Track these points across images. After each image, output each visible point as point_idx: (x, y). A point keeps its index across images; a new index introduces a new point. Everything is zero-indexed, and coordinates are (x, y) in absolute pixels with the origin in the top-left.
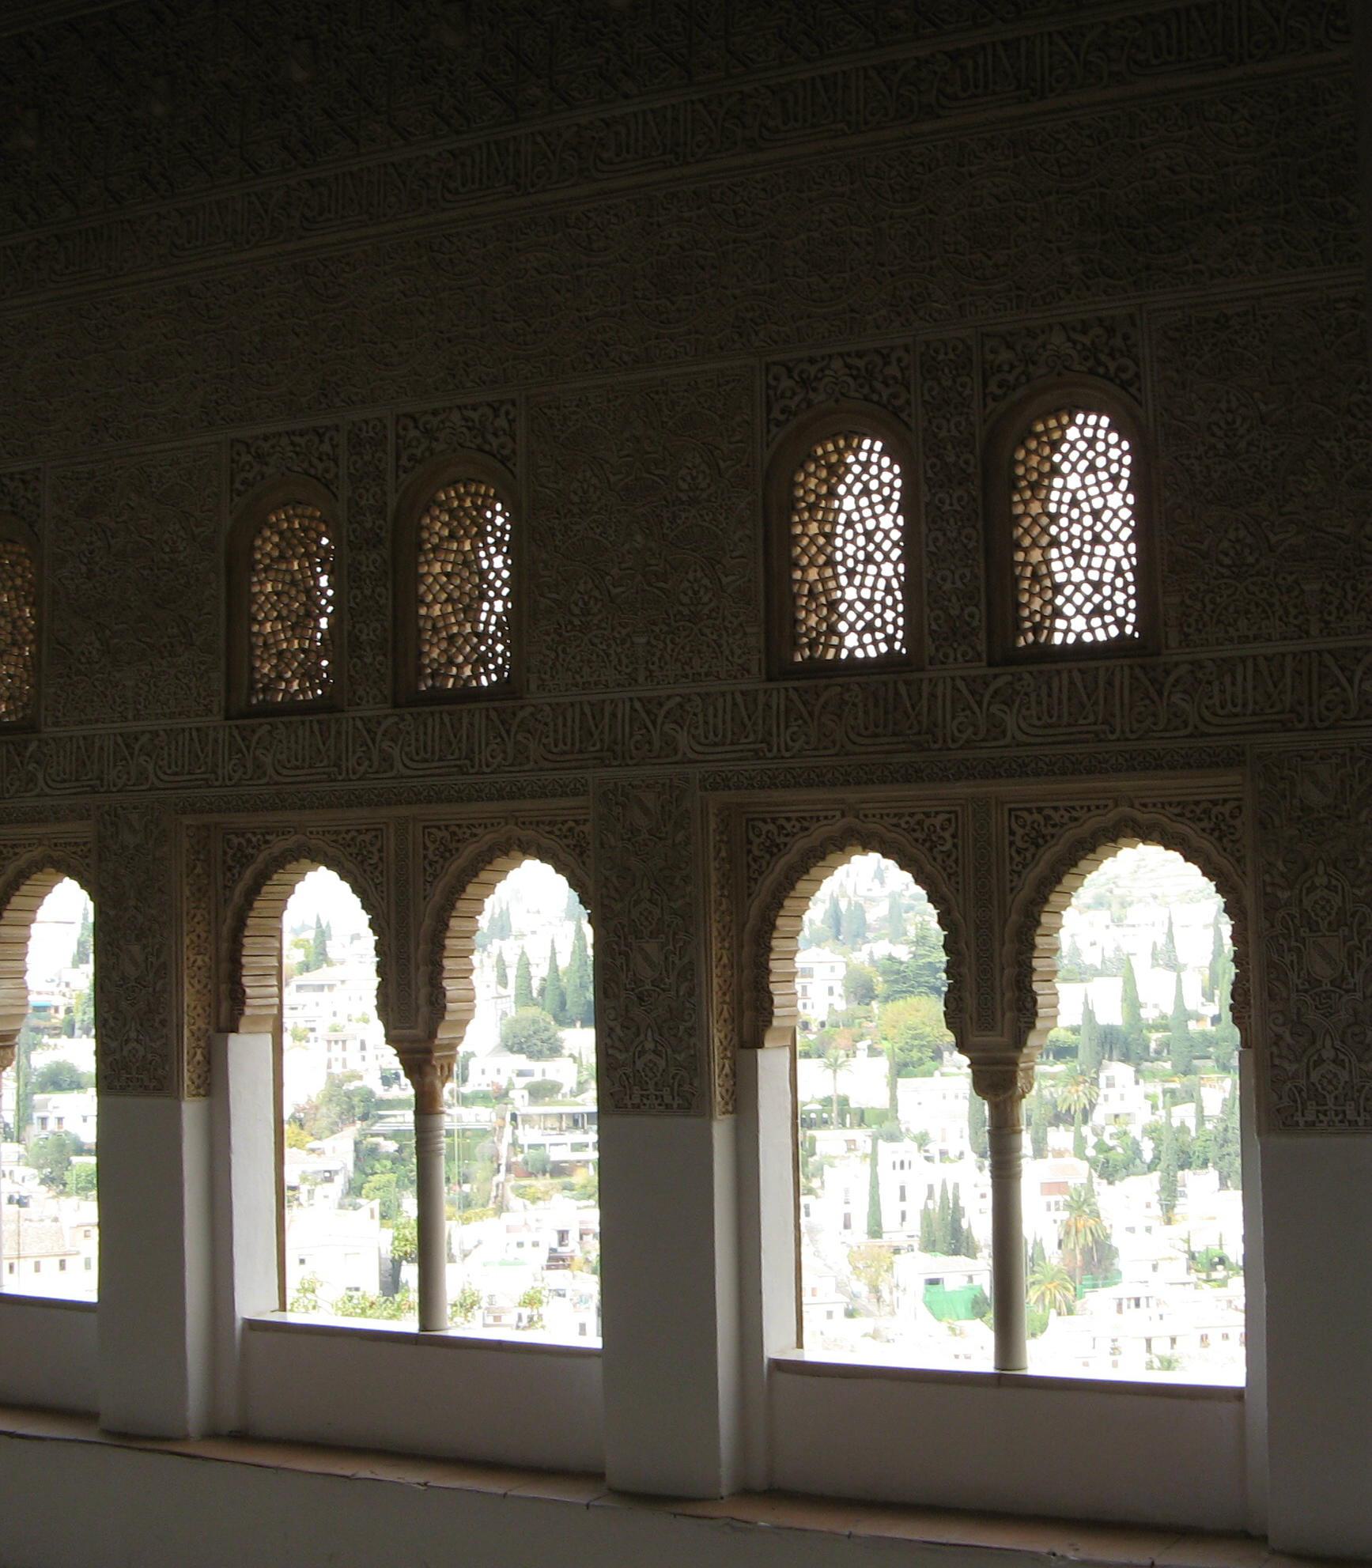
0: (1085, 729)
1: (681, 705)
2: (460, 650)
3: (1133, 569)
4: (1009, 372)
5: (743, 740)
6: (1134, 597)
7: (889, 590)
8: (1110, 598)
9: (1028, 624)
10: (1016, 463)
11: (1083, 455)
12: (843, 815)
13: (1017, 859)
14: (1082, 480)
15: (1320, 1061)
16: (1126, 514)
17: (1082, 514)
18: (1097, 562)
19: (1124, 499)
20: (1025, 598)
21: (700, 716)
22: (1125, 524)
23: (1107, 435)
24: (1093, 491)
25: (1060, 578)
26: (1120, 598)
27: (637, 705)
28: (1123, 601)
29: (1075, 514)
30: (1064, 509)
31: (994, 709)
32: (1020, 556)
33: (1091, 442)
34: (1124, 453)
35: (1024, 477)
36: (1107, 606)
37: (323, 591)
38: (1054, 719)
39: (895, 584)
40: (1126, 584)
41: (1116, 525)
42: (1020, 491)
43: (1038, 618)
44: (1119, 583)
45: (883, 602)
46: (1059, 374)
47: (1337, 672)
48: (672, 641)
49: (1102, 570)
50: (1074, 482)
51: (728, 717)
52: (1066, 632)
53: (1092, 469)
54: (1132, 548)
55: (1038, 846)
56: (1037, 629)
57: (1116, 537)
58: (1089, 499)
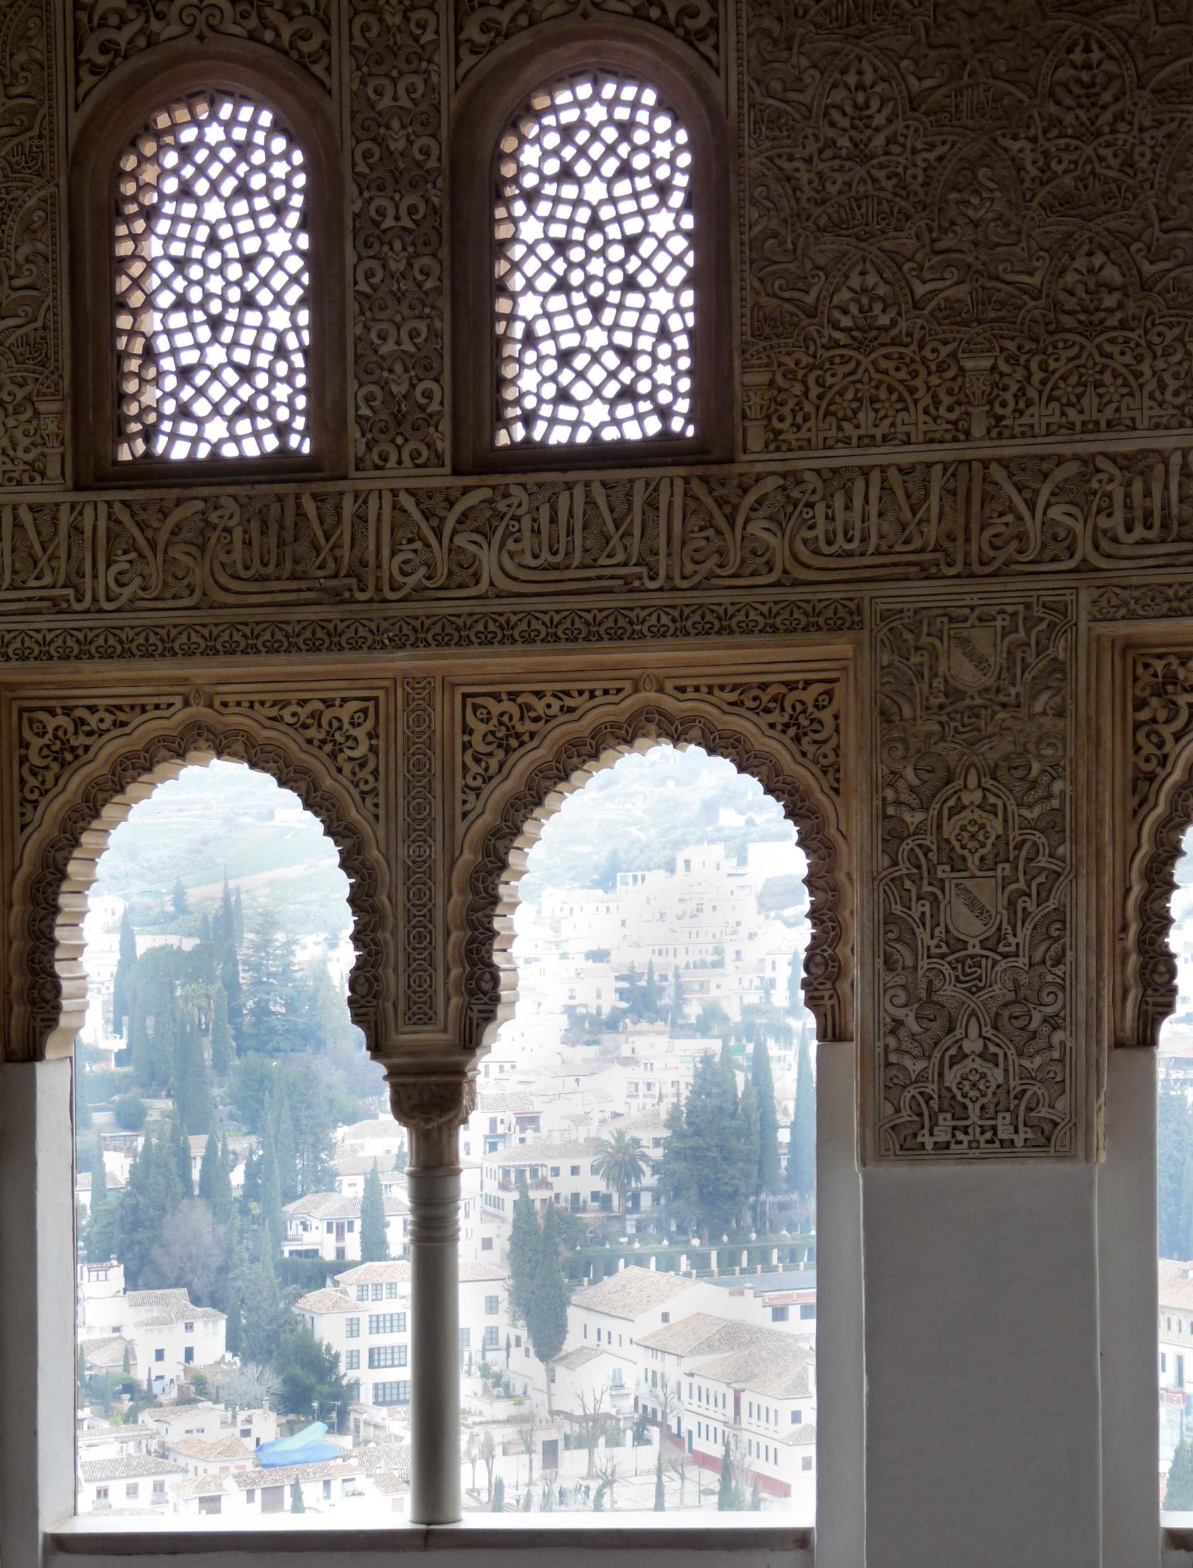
0: (38, 593)
6: (304, 391)
8: (266, 391)
9: (135, 427)
14: (227, 209)
16: (295, 264)
17: (226, 261)
18: (248, 337)
19: (293, 241)
20: (131, 386)
23: (268, 140)
24: (246, 226)
29: (214, 260)
30: (197, 251)
33: (243, 149)
34: (294, 170)
35: (134, 198)
36: (262, 403)
38: (271, 567)
40: (293, 371)
42: (128, 220)
43: (152, 418)
44: (282, 369)
46: (201, 37)
47: (136, 532)
49: (255, 348)
52: (196, 441)
53: (243, 191)
55: (63, 764)
58: (237, 238)
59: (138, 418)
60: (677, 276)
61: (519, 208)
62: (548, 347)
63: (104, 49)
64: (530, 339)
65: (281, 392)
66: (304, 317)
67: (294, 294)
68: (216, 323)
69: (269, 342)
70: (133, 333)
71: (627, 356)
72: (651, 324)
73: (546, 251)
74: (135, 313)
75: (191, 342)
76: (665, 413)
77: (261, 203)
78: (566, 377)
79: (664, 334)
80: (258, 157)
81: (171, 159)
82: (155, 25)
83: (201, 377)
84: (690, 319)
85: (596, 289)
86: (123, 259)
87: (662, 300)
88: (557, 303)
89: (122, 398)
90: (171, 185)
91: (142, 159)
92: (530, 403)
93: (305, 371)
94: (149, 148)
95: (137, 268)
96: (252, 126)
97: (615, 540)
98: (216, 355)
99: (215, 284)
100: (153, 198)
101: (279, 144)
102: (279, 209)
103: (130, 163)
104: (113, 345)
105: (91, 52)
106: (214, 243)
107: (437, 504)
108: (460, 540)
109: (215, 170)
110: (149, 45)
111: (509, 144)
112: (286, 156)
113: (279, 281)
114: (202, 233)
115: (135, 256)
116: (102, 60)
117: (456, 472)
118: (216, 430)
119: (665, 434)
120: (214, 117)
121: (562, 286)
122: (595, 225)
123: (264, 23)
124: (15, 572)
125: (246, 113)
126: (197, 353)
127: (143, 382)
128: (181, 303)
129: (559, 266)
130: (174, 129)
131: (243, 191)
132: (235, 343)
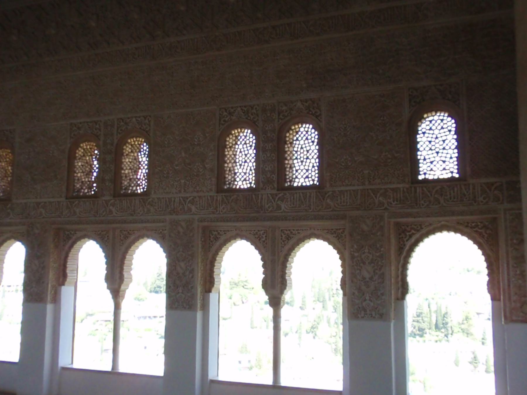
1: (193, 199)
2: (133, 183)
3: (254, 169)
4: (226, 118)
5: (210, 209)
11: (243, 140)
13: (211, 243)
15: (178, 293)
22: (253, 158)
25: (236, 171)
26: (251, 177)
27: (181, 199)
28: (252, 177)
31: (189, 205)
32: (226, 165)
37: (9, 170)
39: (145, 175)
41: (250, 158)
45: (142, 179)
48: (191, 182)
50: (241, 146)
54: (254, 164)
56: (229, 184)
57: (250, 161)
59: (289, 179)
60: (454, 147)
61: (422, 135)
62: (428, 161)
63: (283, 116)
64: (425, 159)
65: (313, 174)
66: (317, 160)
67: (315, 156)
68: (302, 162)
69: (311, 165)
70: (421, 155)
72: (449, 156)
74: (288, 160)
75: (298, 165)
76: (452, 172)
77: (310, 141)
78: (432, 166)
79: (451, 158)
80: (309, 133)
81: (295, 134)
83: (299, 171)
84: (456, 155)
85: (437, 150)
86: (419, 142)
87: (451, 151)
88: (430, 152)
89: (286, 175)
90: (295, 138)
91: (290, 134)
92: (425, 171)
93: (318, 170)
94: (291, 132)
95: (289, 153)
96: (308, 128)
98: (302, 167)
99: (302, 155)
100: (291, 141)
101: (313, 131)
102: (313, 142)
103: (288, 135)
104: (284, 166)
105: (281, 117)
106: (302, 148)
108: (436, 196)
109: (302, 135)
111: (419, 124)
112: (314, 133)
113: (313, 154)
114: (300, 146)
115: (289, 151)
116: (282, 117)
118: (302, 180)
119: (452, 177)
120: (302, 126)
121: (431, 149)
122: (437, 138)
125: (307, 126)
126: (299, 167)
127: (289, 172)
128: (296, 158)
129: (430, 146)
130: (295, 129)
131: (307, 139)
132: (305, 165)
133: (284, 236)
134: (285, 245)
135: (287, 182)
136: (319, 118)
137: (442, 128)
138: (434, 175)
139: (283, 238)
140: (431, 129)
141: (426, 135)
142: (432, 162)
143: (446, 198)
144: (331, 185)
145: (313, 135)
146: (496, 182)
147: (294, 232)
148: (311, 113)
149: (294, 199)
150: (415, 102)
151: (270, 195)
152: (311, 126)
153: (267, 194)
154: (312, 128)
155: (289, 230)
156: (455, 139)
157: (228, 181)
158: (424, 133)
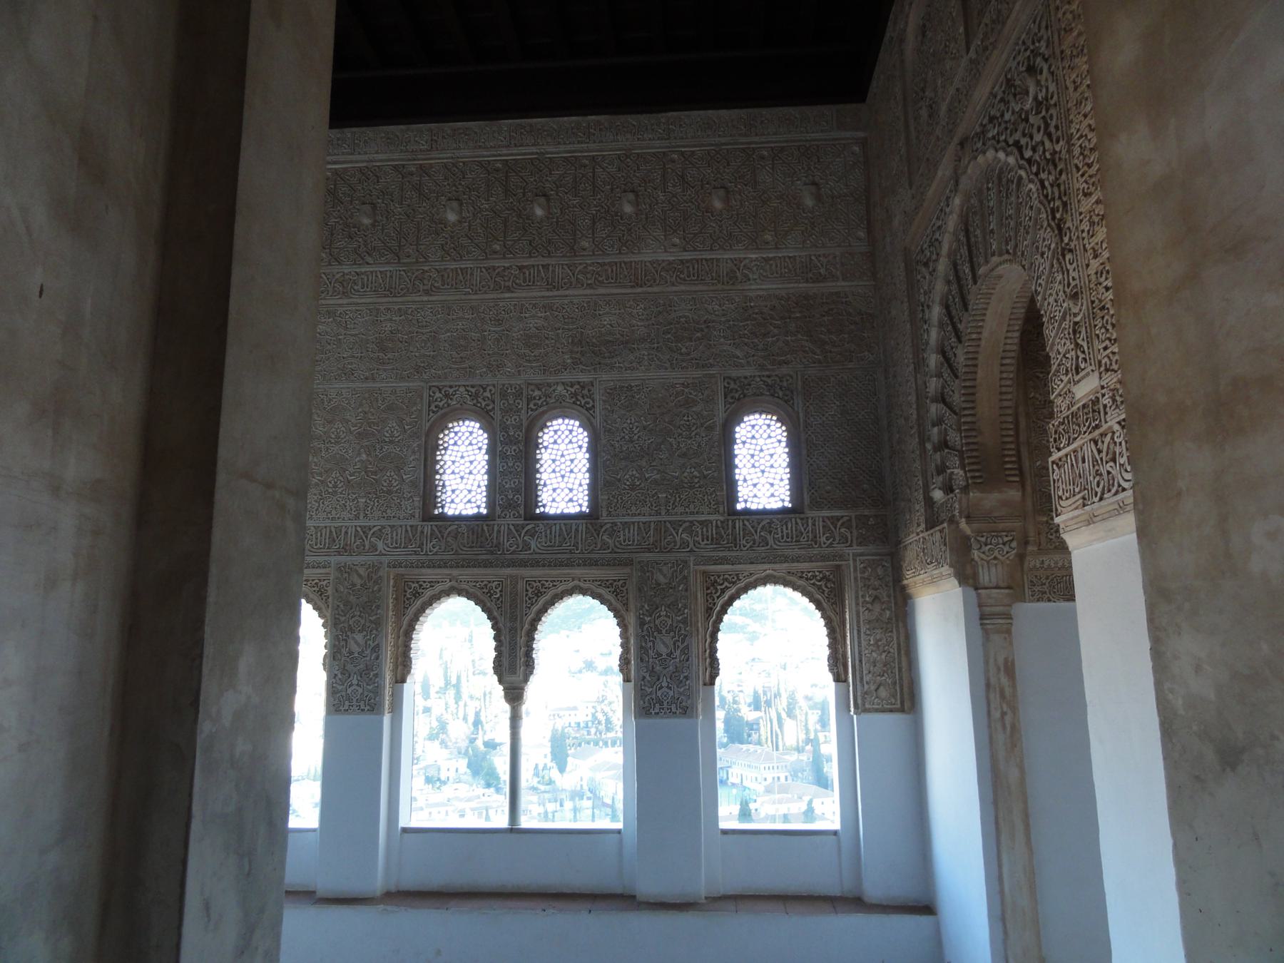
7: (479, 486)
10: (439, 439)
12: (450, 581)
13: (407, 602)
21: (390, 535)
48: (378, 501)
51: (403, 536)
61: (741, 446)
64: (745, 480)
71: (772, 485)
73: (749, 457)
76: (783, 501)
78: (755, 491)
79: (782, 480)
81: (552, 433)
82: (548, 399)
92: (746, 497)
97: (804, 535)
99: (563, 467)
102: (580, 447)
105: (531, 406)
107: (755, 524)
108: (762, 534)
110: (744, 396)
117: (729, 515)
121: (753, 466)
122: (761, 450)
123: (577, 400)
124: (797, 537)
129: (752, 461)
133: (531, 590)
134: (532, 605)
135: (539, 507)
136: (591, 412)
137: (770, 437)
138: (759, 503)
139: (529, 593)
140: (753, 437)
141: (747, 445)
142: (755, 485)
143: (776, 536)
144: (609, 514)
145: (580, 437)
146: (842, 517)
147: (547, 584)
148: (578, 403)
149: (551, 533)
150: (732, 398)
151: (512, 527)
152: (577, 423)
153: (508, 525)
154: (580, 426)
155: (540, 581)
156: (787, 453)
157: (440, 503)
158: (744, 443)
